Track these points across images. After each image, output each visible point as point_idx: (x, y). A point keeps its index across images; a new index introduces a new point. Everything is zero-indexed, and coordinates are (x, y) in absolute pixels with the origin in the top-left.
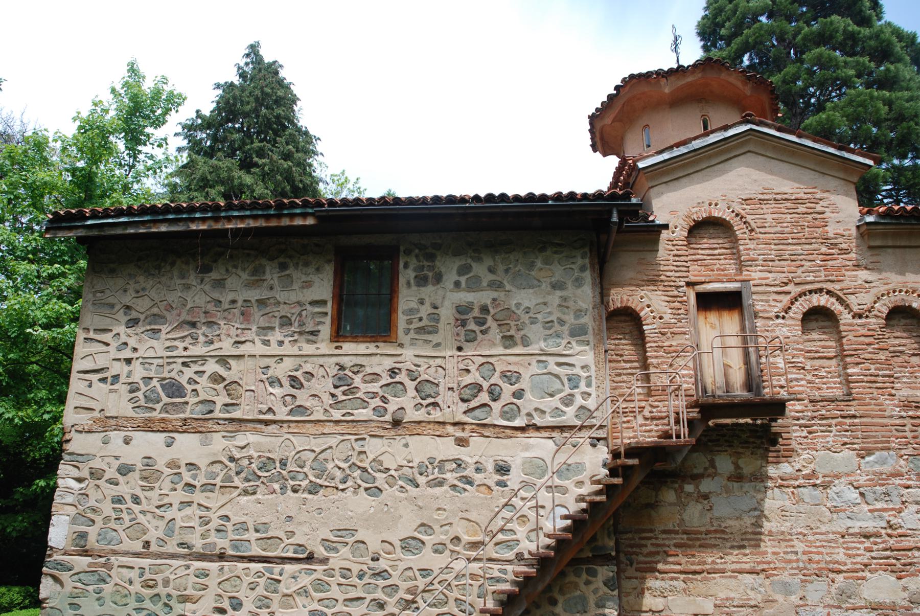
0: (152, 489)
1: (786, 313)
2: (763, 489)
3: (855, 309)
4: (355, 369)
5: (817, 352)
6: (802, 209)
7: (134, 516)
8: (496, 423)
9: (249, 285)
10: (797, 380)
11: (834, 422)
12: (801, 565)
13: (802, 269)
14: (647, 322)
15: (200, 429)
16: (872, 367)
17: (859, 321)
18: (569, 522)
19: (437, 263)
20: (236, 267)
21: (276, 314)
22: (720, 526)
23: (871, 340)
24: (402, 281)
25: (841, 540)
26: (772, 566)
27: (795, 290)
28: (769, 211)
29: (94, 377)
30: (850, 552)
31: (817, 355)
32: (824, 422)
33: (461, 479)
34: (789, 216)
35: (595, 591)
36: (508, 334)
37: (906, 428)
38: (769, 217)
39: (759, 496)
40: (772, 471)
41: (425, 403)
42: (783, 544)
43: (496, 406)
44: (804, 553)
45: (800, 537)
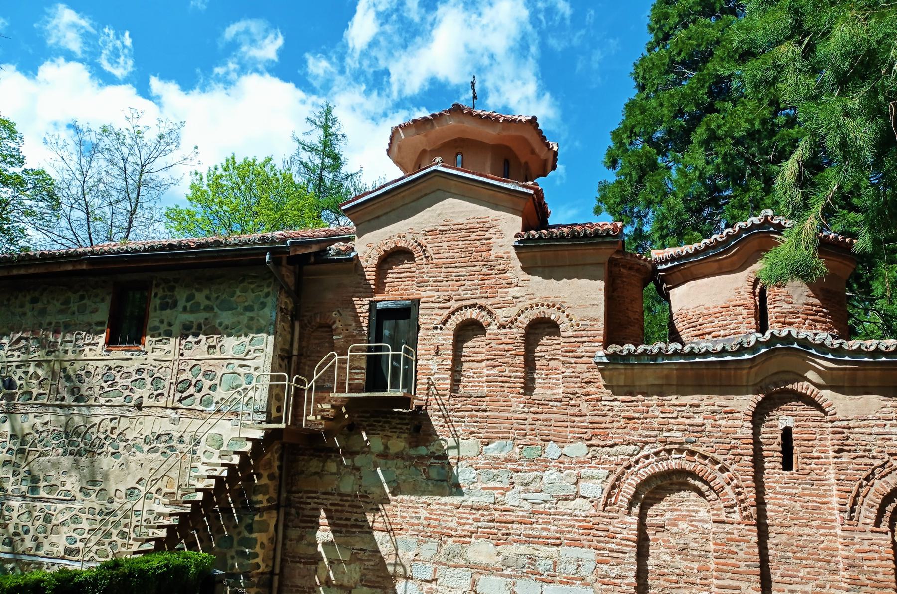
1: (444, 324)
2: (402, 466)
3: (502, 320)
4: (118, 369)
5: (469, 356)
6: (473, 236)
8: (197, 408)
9: (61, 312)
10: (443, 379)
11: (467, 414)
12: (421, 528)
13: (463, 288)
14: (339, 331)
16: (507, 369)
17: (503, 331)
18: (213, 482)
19: (176, 293)
20: (53, 299)
22: (366, 492)
23: (511, 346)
24: (152, 306)
25: (455, 511)
26: (399, 527)
27: (454, 305)
28: (446, 239)
30: (461, 521)
31: (468, 359)
32: (461, 414)
33: (168, 448)
34: (461, 243)
35: (239, 533)
36: (212, 344)
37: (526, 422)
38: (445, 245)
39: (398, 472)
40: (412, 452)
41: (156, 393)
42: (411, 510)
43: (198, 396)
44: (426, 519)
45: (425, 505)
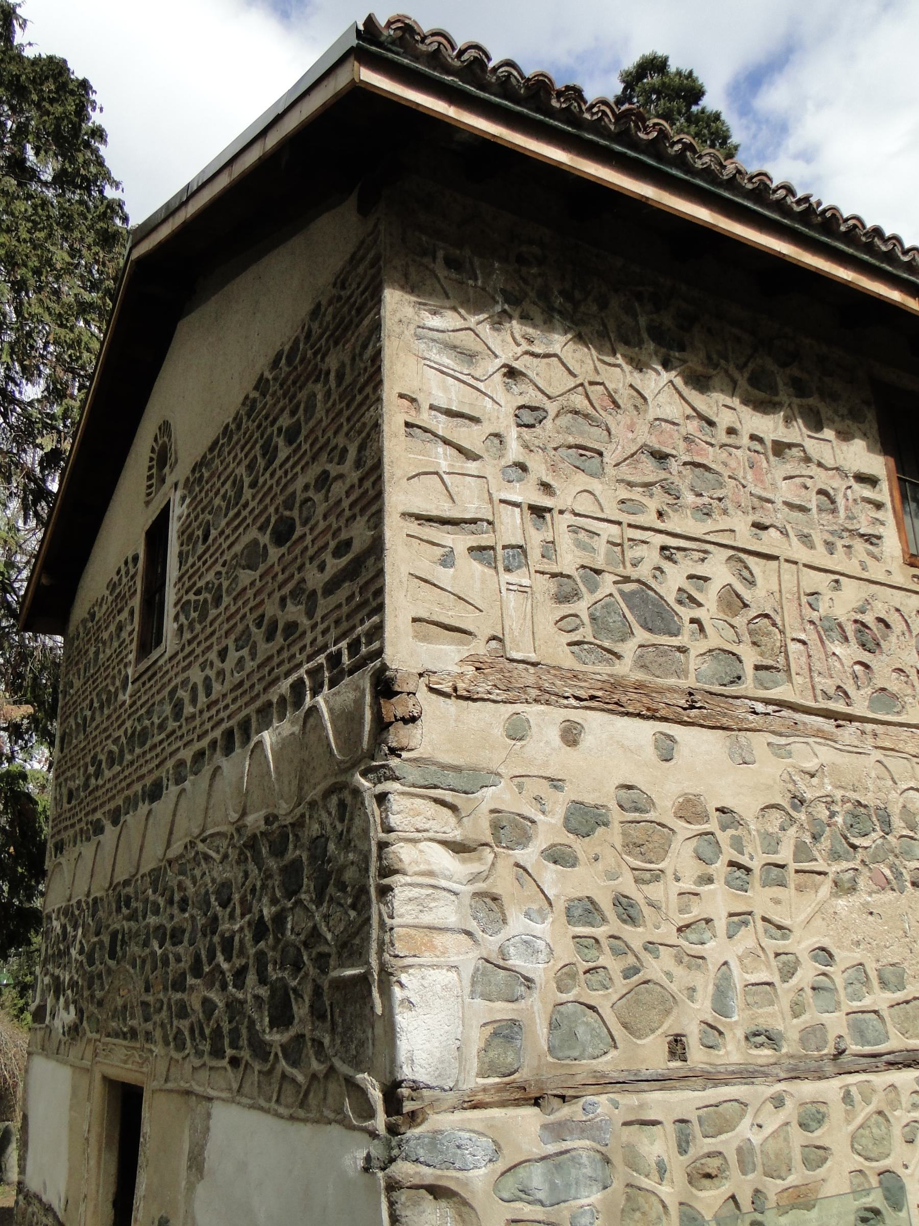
0: (658, 876)
7: (631, 960)
15: (725, 721)
21: (809, 483)
29: (459, 541)
